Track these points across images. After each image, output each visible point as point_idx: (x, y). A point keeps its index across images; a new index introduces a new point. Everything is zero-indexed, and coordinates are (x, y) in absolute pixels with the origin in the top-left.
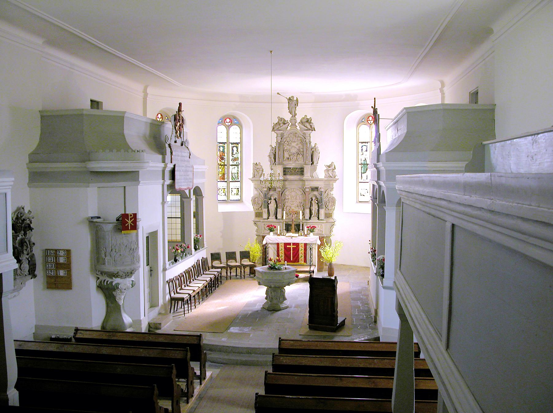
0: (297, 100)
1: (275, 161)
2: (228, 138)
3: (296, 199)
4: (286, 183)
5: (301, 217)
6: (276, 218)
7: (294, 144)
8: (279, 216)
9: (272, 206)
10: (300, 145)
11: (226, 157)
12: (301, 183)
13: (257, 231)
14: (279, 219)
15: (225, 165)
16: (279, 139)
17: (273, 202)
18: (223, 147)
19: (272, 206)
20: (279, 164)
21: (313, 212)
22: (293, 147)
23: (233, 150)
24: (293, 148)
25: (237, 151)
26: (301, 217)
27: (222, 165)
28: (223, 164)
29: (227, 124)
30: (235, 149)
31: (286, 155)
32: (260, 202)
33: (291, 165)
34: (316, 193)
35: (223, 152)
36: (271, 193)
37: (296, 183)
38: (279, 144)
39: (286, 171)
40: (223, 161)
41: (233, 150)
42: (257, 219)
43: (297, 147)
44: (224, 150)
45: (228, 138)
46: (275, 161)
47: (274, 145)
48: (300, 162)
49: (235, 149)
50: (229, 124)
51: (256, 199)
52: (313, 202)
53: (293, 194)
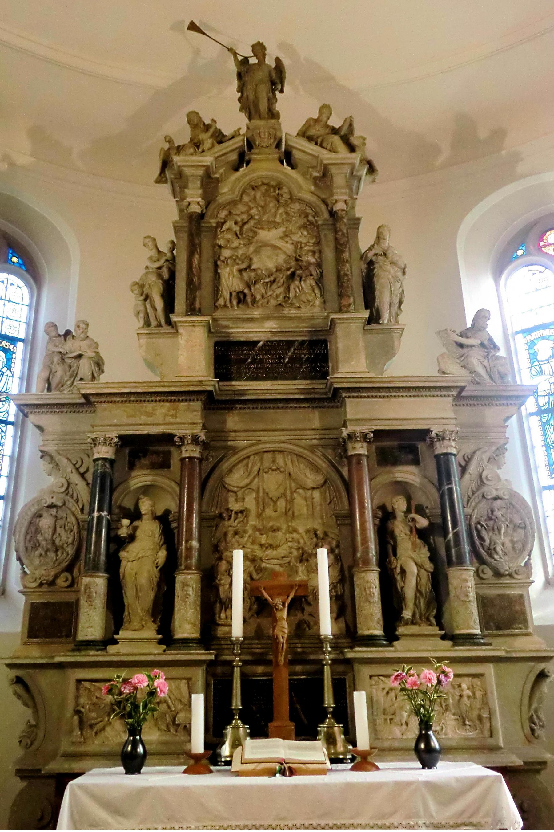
0: (279, 68)
1: (169, 308)
4: (233, 421)
5: (326, 626)
6: (167, 638)
8: (186, 621)
9: (142, 559)
10: (301, 236)
12: (314, 419)
13: (30, 738)
14: (185, 642)
16: (194, 198)
17: (148, 531)
19: (142, 559)
20: (192, 310)
21: (409, 589)
22: (265, 245)
24: (267, 251)
26: (326, 626)
31: (230, 281)
32: (66, 537)
33: (257, 327)
34: (407, 474)
36: (140, 478)
37: (287, 418)
38: (195, 227)
39: (228, 356)
42: (35, 654)
46: (169, 308)
47: (166, 236)
48: (305, 312)
51: (46, 522)
52: (400, 529)
53: (272, 483)
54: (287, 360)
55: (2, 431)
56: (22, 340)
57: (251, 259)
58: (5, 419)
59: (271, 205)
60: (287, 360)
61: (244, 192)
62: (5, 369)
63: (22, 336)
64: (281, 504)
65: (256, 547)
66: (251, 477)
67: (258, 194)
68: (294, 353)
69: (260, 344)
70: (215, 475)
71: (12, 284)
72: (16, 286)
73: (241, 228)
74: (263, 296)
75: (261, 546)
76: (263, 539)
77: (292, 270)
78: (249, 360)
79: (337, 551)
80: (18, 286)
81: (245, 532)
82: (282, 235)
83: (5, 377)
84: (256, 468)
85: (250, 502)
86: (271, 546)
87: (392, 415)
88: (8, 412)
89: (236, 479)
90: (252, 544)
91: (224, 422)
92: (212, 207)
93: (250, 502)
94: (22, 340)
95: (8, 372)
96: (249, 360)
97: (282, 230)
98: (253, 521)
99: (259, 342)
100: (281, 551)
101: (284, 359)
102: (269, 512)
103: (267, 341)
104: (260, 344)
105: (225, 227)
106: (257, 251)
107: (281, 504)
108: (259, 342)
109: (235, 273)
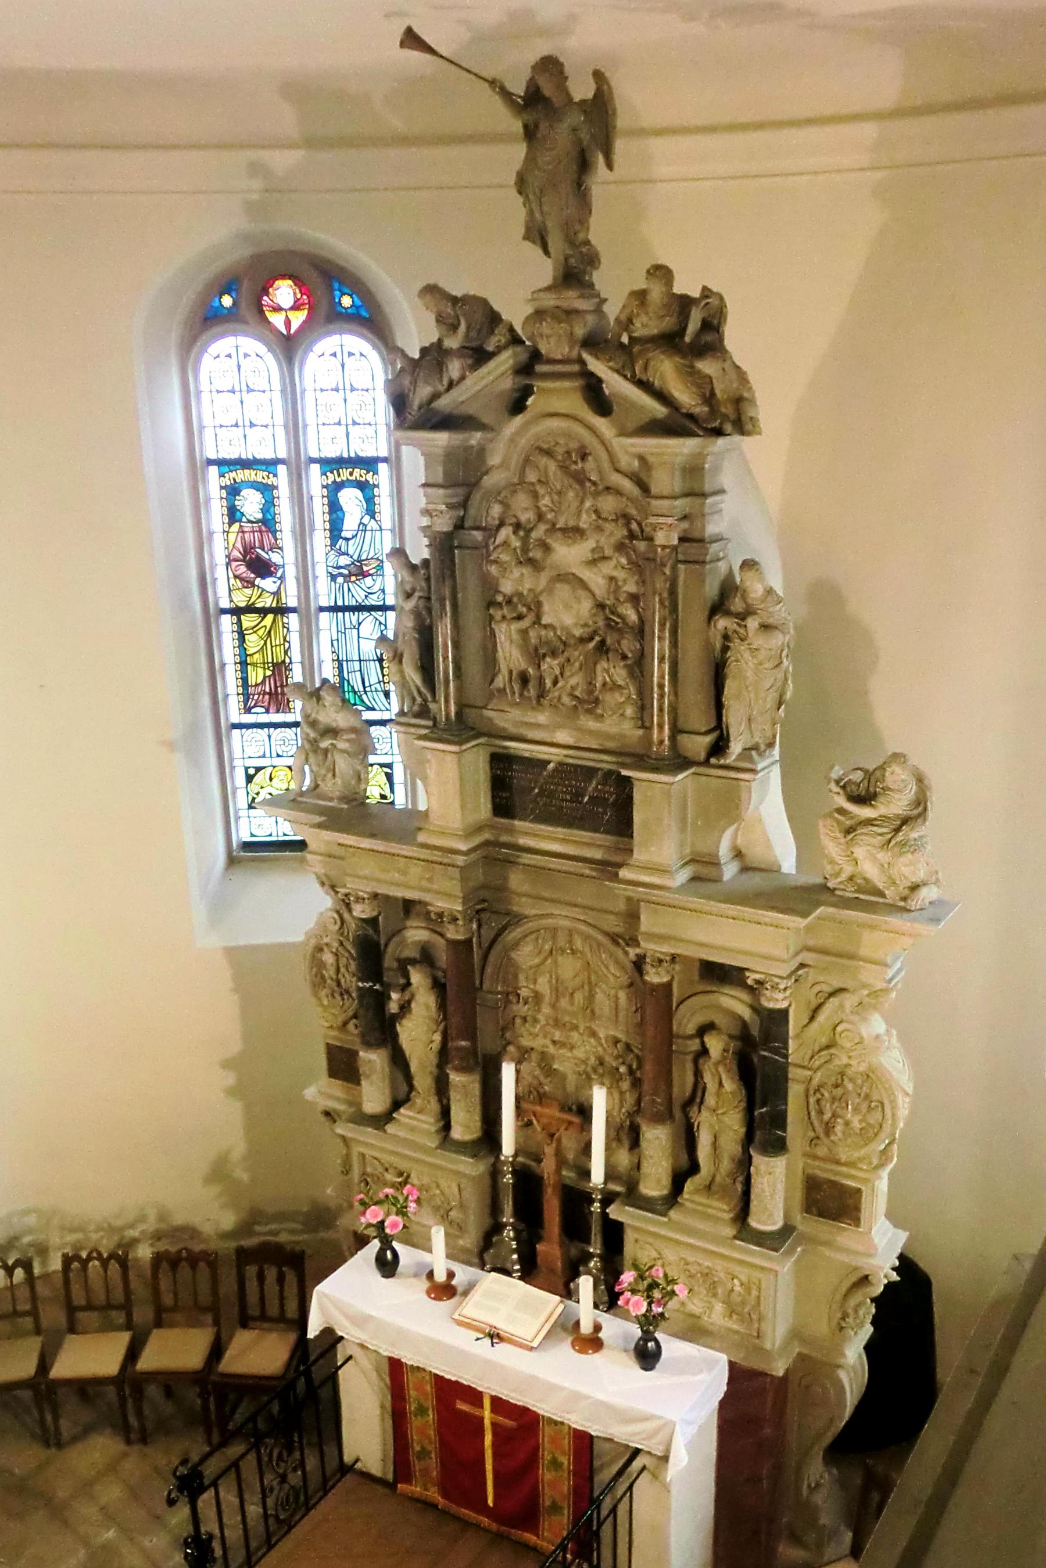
2: (294, 427)
3: (589, 1008)
7: (569, 555)
11: (286, 557)
15: (281, 611)
18: (267, 490)
22: (564, 577)
23: (334, 508)
25: (371, 513)
27: (264, 612)
28: (268, 602)
29: (277, 320)
30: (350, 499)
33: (549, 737)
35: (268, 523)
40: (268, 584)
41: (334, 508)
43: (596, 580)
44: (269, 505)
45: (294, 427)
49: (350, 499)
50: (298, 318)
53: (568, 968)
54: (586, 799)
55: (380, 623)
56: (385, 460)
57: (539, 604)
58: (381, 603)
59: (571, 494)
60: (586, 799)
61: (527, 461)
62: (367, 517)
63: (383, 453)
64: (579, 997)
65: (548, 1042)
66: (542, 957)
67: (552, 466)
68: (596, 789)
69: (551, 766)
70: (498, 948)
71: (350, 354)
72: (358, 355)
73: (525, 541)
74: (555, 682)
75: (554, 1042)
76: (557, 1035)
77: (597, 638)
78: (536, 791)
79: (638, 1074)
80: (361, 355)
81: (536, 1021)
82: (590, 556)
83: (368, 534)
84: (547, 947)
85: (543, 985)
86: (563, 1045)
87: (701, 937)
88: (383, 591)
89: (525, 956)
90: (545, 1037)
91: (506, 879)
92: (477, 497)
93: (543, 985)
94: (385, 460)
95: (373, 524)
96: (536, 791)
97: (591, 544)
98: (546, 1010)
99: (549, 762)
100: (579, 1053)
101: (583, 796)
102: (564, 1003)
103: (561, 764)
104: (551, 766)
105: (499, 539)
106: (549, 590)
107: (579, 997)
108: (549, 762)
109: (515, 636)
